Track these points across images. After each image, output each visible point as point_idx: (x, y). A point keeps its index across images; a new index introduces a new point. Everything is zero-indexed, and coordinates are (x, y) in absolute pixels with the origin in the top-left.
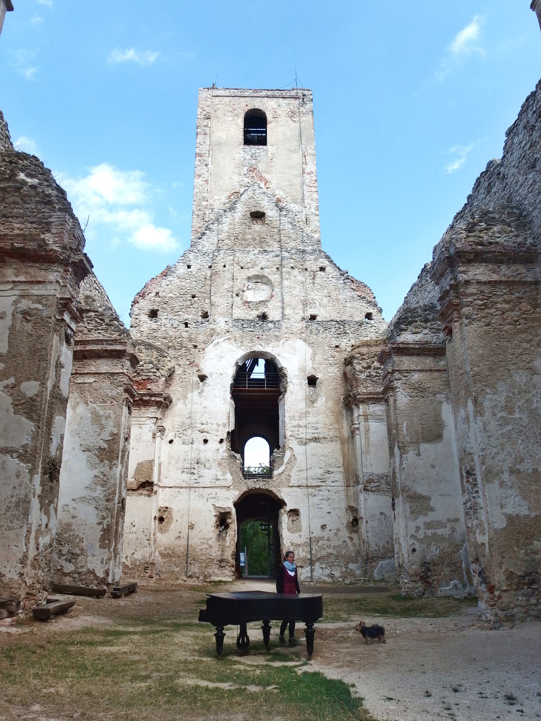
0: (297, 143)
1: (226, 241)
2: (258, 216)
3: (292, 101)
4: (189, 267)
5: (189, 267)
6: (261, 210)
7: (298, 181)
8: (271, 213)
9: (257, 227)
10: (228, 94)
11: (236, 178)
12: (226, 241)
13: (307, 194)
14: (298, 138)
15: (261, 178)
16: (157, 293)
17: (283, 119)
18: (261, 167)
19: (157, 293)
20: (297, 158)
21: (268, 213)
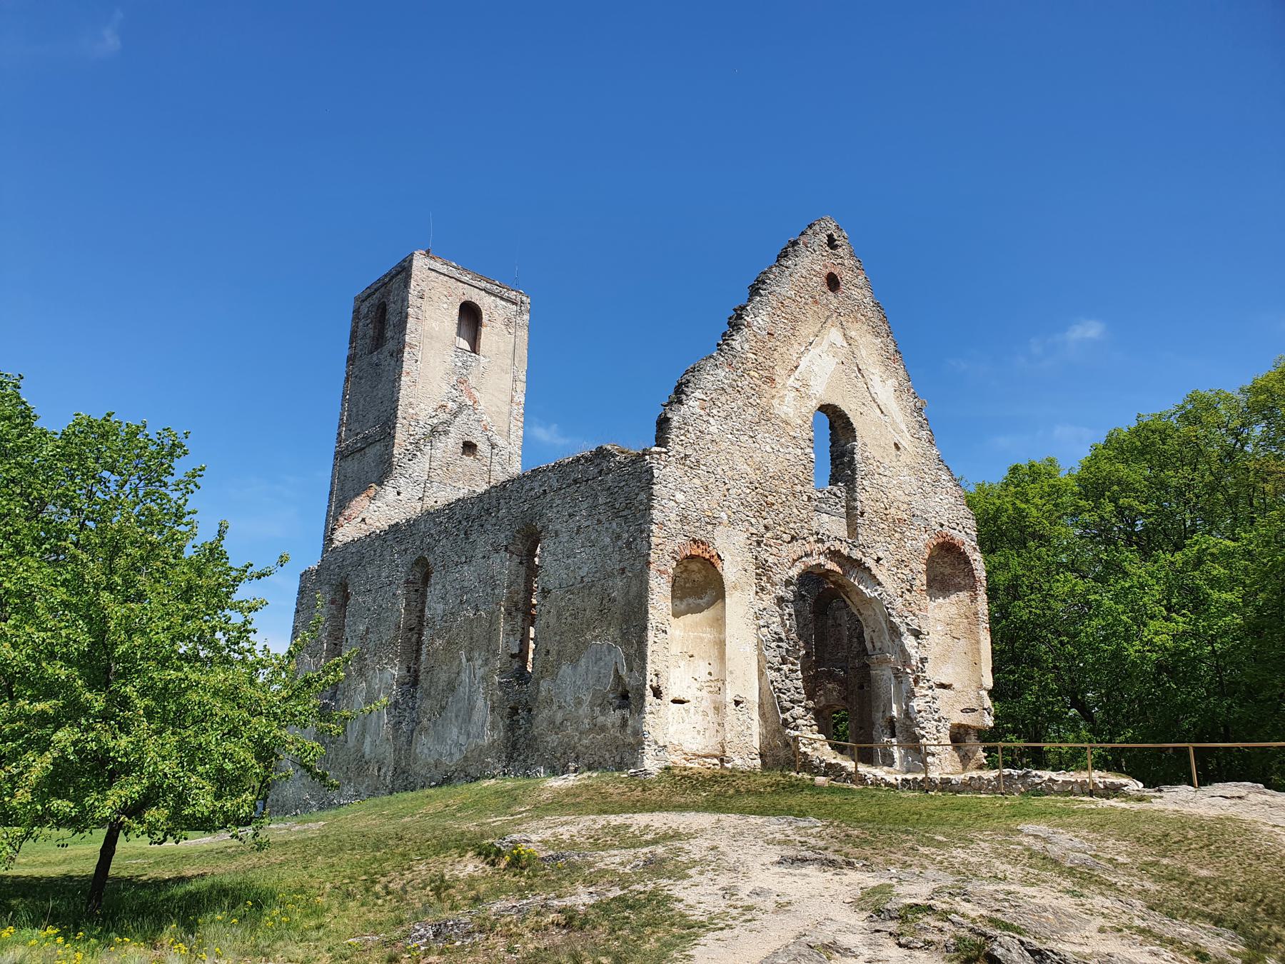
0: (509, 362)
1: (439, 471)
2: (469, 448)
3: (509, 305)
4: (399, 494)
5: (399, 494)
6: (474, 441)
7: (506, 409)
8: (483, 447)
9: (468, 460)
10: (445, 271)
11: (446, 388)
12: (439, 471)
13: (513, 429)
14: (511, 356)
15: (471, 396)
16: (363, 520)
17: (499, 325)
18: (472, 381)
19: (363, 520)
20: (509, 377)
21: (480, 446)
